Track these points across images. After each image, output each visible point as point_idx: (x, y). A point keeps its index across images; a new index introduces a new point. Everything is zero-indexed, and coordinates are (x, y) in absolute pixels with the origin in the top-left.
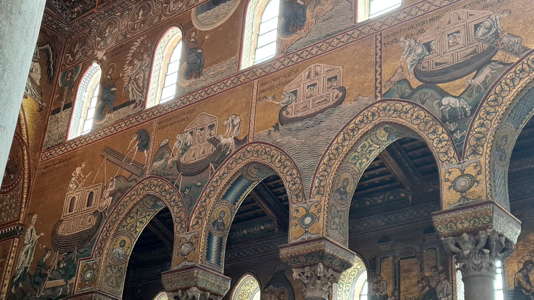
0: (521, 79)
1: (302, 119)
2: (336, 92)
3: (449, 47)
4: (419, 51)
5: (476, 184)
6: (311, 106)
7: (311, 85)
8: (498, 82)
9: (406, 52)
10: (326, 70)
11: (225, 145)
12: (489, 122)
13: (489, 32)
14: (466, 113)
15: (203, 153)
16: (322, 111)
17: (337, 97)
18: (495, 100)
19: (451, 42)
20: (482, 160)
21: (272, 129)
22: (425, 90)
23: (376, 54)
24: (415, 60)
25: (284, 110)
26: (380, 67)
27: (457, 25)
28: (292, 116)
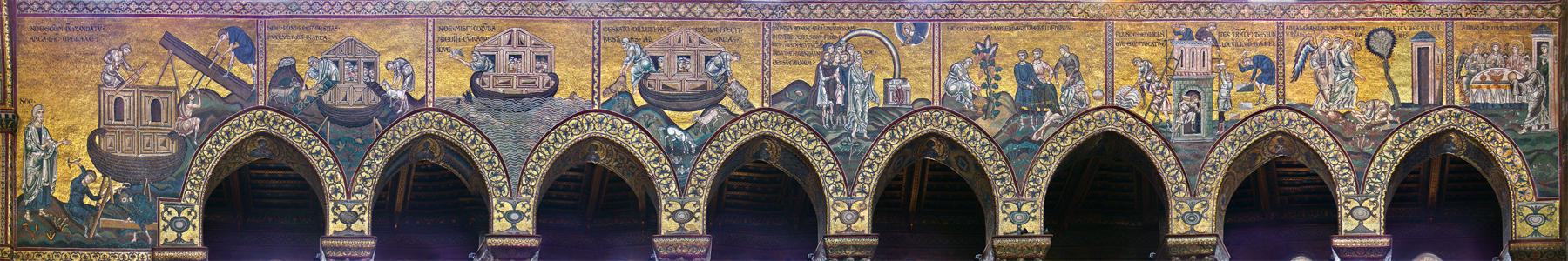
0: (742, 134)
1: (505, 97)
2: (548, 78)
3: (679, 71)
4: (646, 63)
5: (694, 219)
6: (515, 84)
7: (515, 56)
8: (722, 130)
9: (630, 59)
10: (533, 42)
11: (393, 100)
12: (711, 167)
13: (718, 71)
14: (691, 150)
15: (361, 99)
16: (530, 96)
17: (548, 84)
18: (718, 147)
19: (680, 65)
20: (702, 201)
21: (462, 97)
22: (650, 112)
23: (594, 48)
24: (640, 72)
25: (477, 77)
26: (599, 66)
27: (687, 49)
28: (489, 89)
